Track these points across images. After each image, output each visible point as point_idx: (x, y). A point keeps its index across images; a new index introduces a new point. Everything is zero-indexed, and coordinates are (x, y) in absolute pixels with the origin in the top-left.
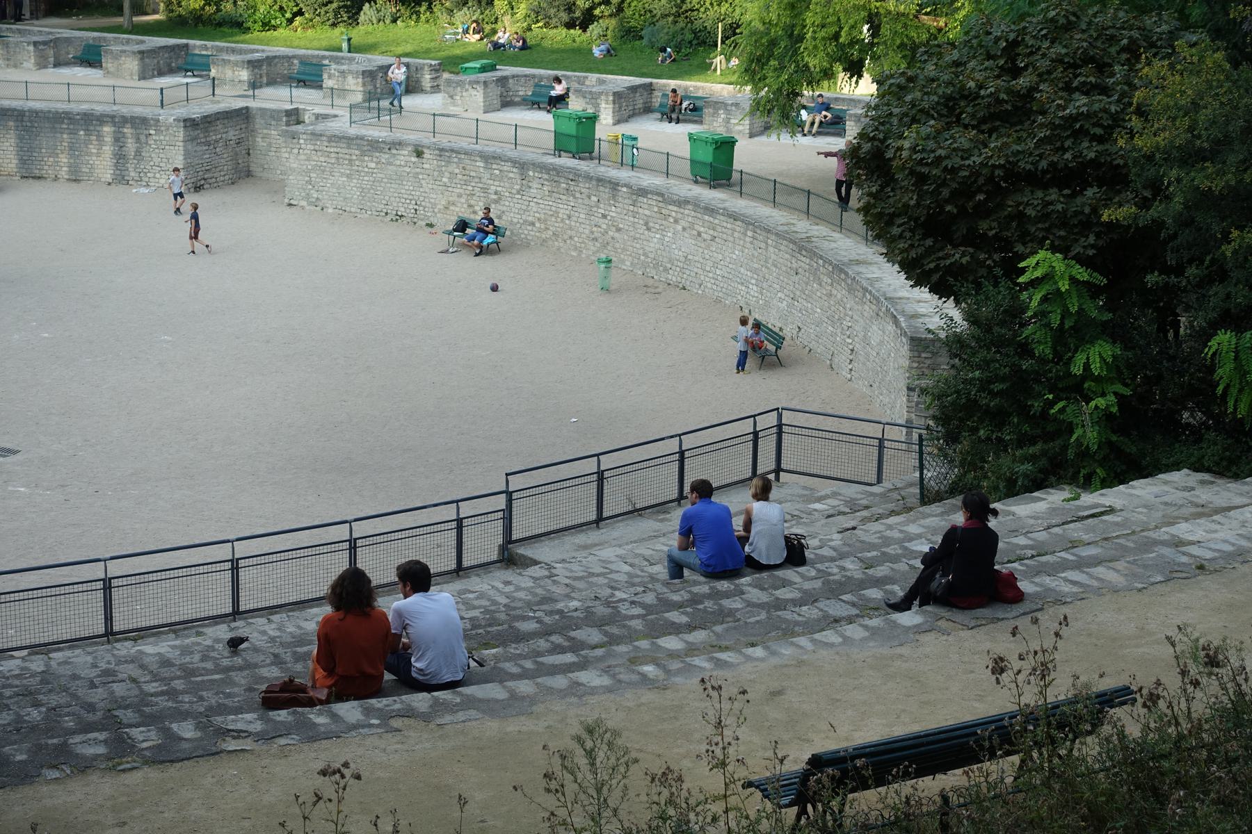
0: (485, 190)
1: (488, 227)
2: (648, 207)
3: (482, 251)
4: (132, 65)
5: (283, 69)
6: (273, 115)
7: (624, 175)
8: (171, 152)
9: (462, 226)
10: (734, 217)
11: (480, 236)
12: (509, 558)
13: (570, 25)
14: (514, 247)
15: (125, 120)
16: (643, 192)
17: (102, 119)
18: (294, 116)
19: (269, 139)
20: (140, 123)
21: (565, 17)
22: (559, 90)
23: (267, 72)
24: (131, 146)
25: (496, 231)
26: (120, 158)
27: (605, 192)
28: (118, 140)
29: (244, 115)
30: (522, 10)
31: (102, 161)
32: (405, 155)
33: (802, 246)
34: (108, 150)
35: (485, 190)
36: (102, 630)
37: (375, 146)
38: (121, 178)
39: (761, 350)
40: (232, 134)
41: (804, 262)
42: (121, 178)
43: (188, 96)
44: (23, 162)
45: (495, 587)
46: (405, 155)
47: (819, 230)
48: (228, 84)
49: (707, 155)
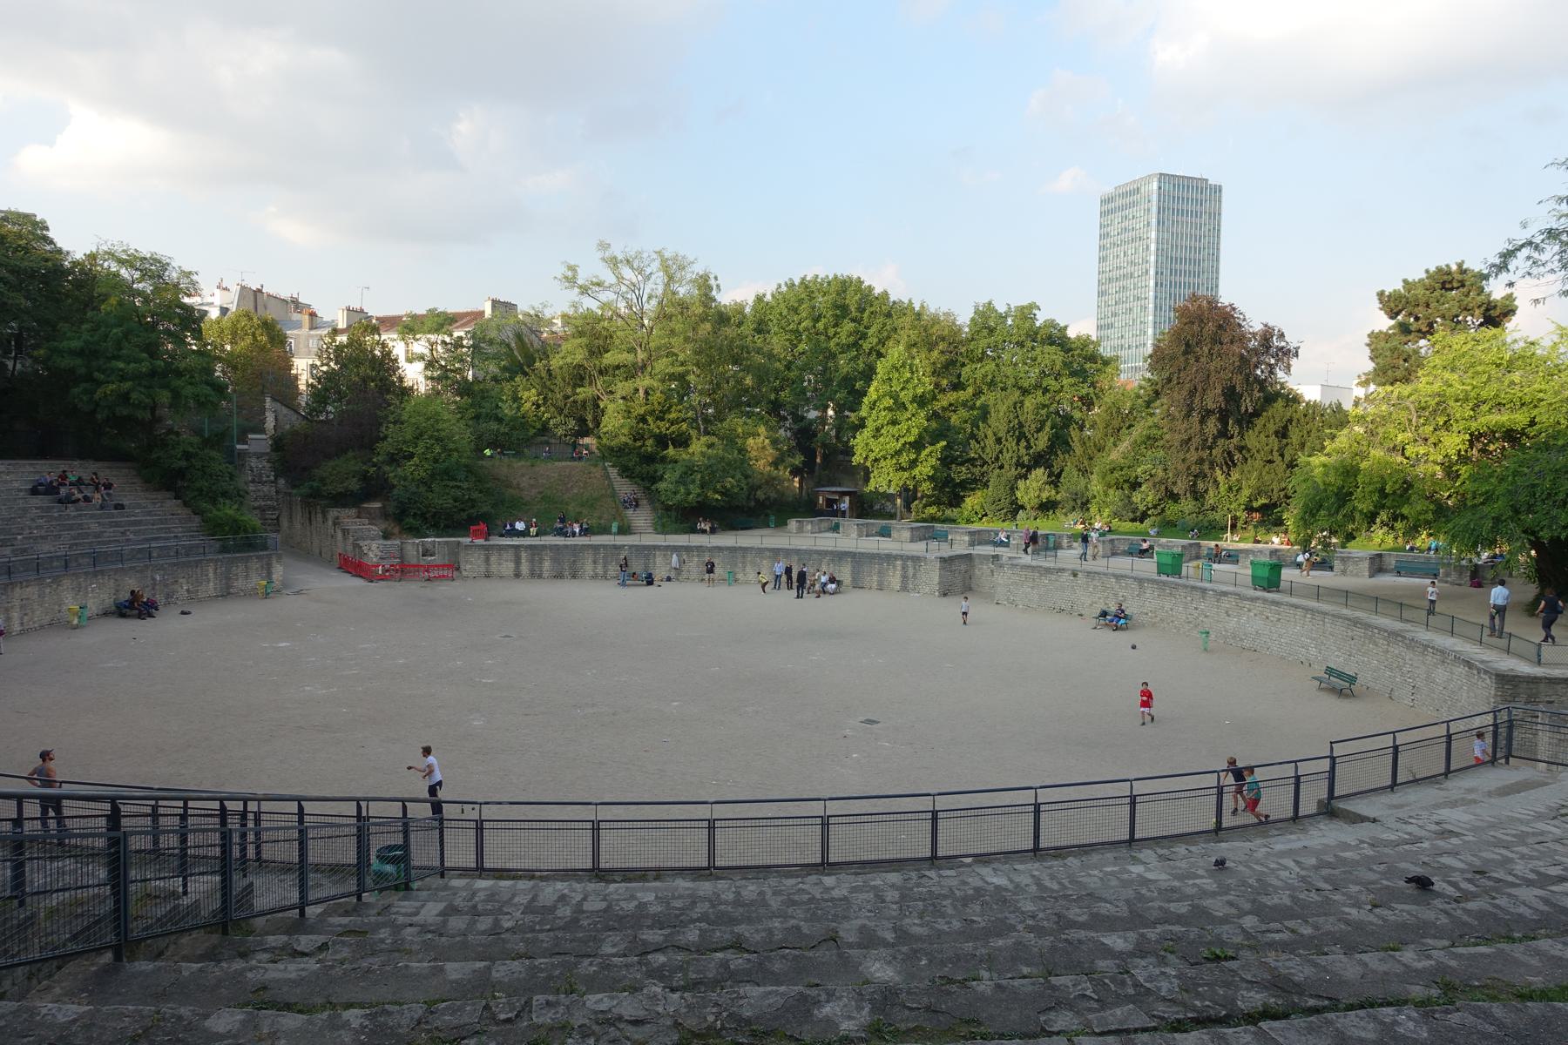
0: (1116, 595)
1: (1121, 615)
2: (1226, 603)
3: (1117, 629)
4: (907, 534)
5: (985, 537)
6: (986, 557)
7: (1207, 585)
8: (932, 576)
9: (1104, 614)
10: (1297, 607)
11: (1116, 619)
12: (1329, 810)
13: (1133, 520)
14: (1134, 628)
15: (908, 558)
16: (1225, 594)
17: (896, 557)
18: (996, 557)
19: (982, 571)
20: (916, 559)
21: (1131, 515)
22: (1145, 546)
23: (977, 538)
24: (911, 571)
25: (1126, 617)
26: (904, 577)
27: (1197, 595)
28: (904, 568)
29: (969, 557)
30: (1107, 512)
31: (895, 580)
32: (1066, 576)
33: (1356, 622)
34: (898, 573)
35: (1116, 595)
36: (1031, 846)
37: (1048, 571)
38: (904, 588)
39: (1341, 685)
40: (963, 567)
41: (1359, 632)
42: (904, 588)
43: (935, 550)
44: (854, 579)
45: (1328, 835)
46: (1066, 576)
47: (1358, 614)
48: (959, 543)
49: (1265, 572)
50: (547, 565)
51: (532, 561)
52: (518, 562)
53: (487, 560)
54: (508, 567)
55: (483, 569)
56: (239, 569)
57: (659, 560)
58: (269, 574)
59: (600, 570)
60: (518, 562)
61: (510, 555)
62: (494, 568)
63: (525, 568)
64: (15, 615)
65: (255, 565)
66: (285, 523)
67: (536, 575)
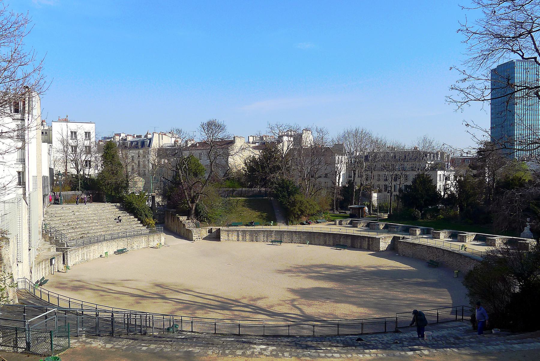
24: (371, 243)
28: (369, 241)
34: (367, 243)
50: (248, 237)
51: (243, 236)
52: (238, 236)
53: (228, 235)
54: (235, 237)
55: (227, 238)
56: (151, 239)
57: (285, 236)
58: (160, 240)
59: (265, 239)
60: (238, 236)
61: (235, 234)
62: (230, 238)
63: (241, 238)
64: (92, 254)
65: (156, 237)
66: (166, 221)
67: (244, 240)
